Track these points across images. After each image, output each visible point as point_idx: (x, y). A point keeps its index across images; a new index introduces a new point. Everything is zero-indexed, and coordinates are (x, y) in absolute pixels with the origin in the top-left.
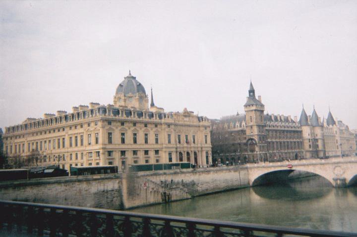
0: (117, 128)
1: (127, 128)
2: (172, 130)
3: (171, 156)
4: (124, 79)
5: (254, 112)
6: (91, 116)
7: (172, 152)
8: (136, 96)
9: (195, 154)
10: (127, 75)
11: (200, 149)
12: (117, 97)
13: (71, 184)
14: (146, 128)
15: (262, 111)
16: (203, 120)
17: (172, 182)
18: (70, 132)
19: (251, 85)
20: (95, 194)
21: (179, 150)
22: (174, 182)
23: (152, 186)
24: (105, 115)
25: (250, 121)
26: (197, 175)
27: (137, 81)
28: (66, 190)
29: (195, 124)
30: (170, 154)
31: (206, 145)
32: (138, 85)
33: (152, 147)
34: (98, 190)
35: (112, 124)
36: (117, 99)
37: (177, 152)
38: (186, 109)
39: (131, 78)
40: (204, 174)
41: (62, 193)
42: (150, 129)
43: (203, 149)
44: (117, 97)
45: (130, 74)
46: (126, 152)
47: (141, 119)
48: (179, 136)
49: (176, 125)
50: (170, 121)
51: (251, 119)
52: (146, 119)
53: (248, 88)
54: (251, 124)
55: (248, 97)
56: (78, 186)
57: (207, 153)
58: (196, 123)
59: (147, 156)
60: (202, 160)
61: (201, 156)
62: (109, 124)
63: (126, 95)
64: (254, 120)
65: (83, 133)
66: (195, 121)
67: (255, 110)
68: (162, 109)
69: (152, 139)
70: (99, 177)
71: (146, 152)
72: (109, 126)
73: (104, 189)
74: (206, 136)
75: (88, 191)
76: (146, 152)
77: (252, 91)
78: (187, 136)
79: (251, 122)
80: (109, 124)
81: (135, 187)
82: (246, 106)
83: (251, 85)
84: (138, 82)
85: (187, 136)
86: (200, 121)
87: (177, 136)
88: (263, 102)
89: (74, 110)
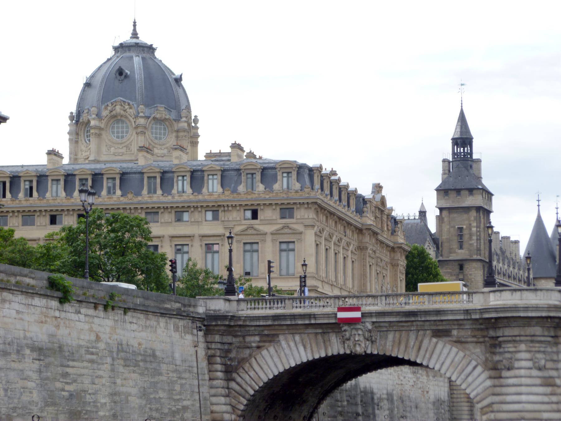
5: (473, 213)
6: (261, 187)
8: (178, 120)
15: (488, 212)
19: (462, 119)
25: (455, 245)
39: (135, 48)
44: (105, 113)
45: (135, 35)
51: (461, 236)
53: (451, 130)
54: (461, 254)
55: (449, 162)
64: (474, 242)
66: (386, 229)
67: (479, 209)
77: (463, 140)
79: (461, 247)
82: (443, 191)
83: (462, 119)
88: (487, 182)
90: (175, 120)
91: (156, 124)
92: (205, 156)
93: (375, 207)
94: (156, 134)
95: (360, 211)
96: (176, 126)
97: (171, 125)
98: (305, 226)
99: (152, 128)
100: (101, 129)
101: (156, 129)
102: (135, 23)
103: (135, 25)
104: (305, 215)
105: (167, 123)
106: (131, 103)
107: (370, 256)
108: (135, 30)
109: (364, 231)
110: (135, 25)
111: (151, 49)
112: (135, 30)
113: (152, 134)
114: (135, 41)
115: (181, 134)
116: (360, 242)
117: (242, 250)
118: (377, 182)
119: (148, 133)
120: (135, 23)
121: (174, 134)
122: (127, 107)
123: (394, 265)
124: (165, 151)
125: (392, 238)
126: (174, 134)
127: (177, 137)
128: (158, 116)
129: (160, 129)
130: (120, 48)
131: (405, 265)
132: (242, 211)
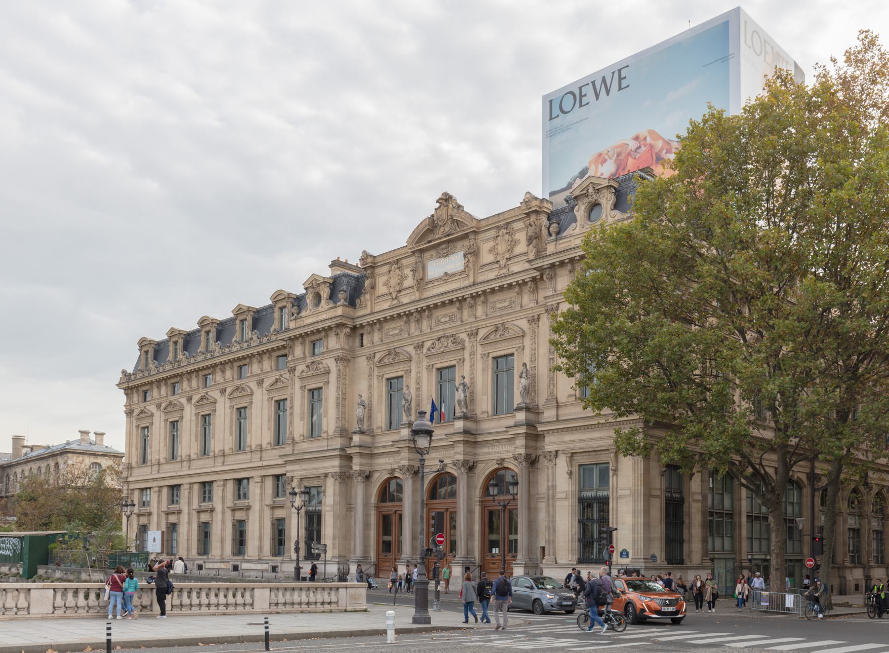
2: (331, 363)
43: (550, 444)
66: (521, 248)
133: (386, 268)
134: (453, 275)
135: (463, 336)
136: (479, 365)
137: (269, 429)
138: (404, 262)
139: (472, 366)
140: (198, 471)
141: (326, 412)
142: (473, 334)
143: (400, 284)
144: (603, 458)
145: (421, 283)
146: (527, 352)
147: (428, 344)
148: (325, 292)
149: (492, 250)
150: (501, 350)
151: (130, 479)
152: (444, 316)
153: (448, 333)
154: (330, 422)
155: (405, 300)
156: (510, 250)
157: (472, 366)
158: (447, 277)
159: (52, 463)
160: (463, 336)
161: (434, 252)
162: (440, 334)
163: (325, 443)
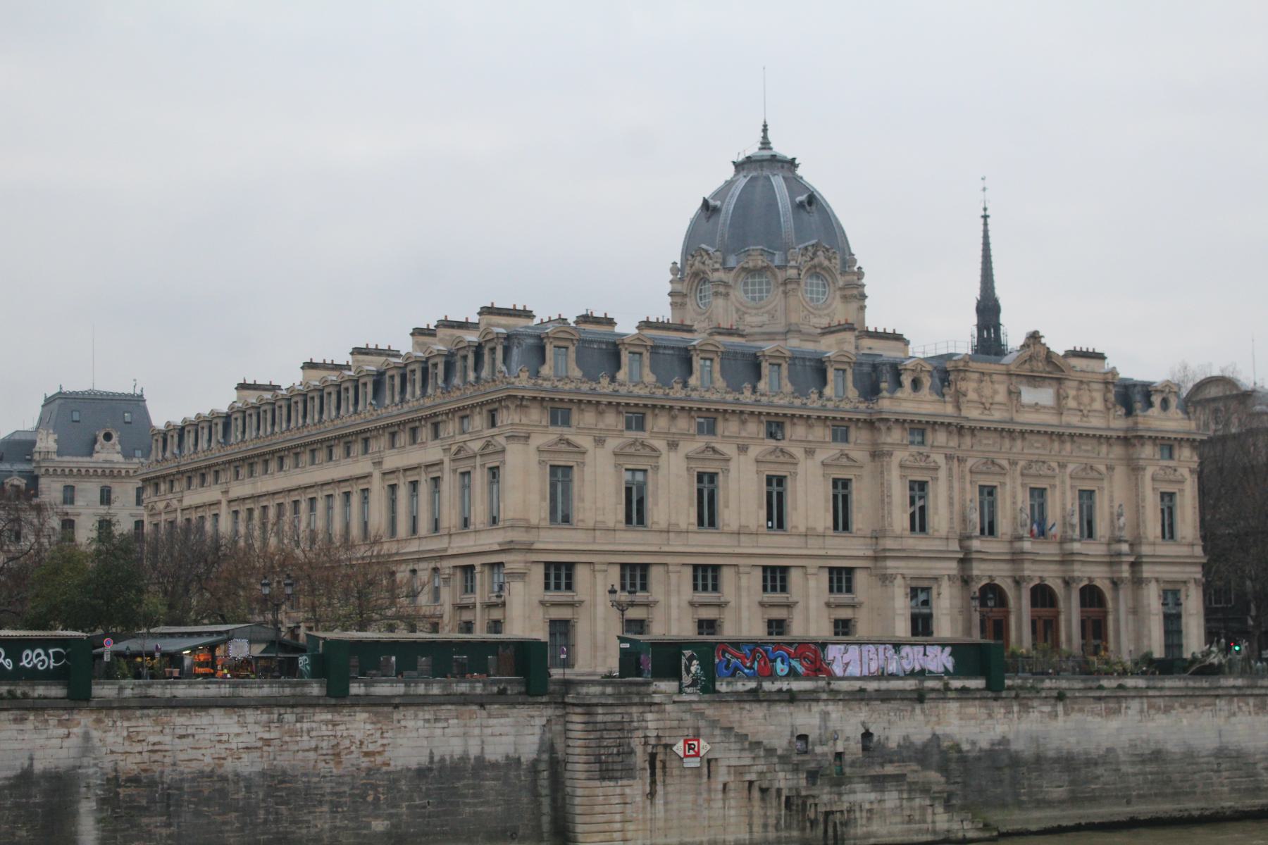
0: (600, 441)
1: (660, 444)
2: (939, 458)
3: (926, 603)
4: (730, 172)
7: (936, 579)
9: (1091, 596)
10: (753, 149)
11: (1125, 572)
12: (687, 270)
13: (289, 717)
14: (773, 443)
16: (1150, 404)
17: (865, 748)
18: (393, 460)
20: (422, 773)
21: (977, 569)
22: (881, 745)
23: (730, 756)
24: (537, 374)
26: (1034, 715)
27: (798, 180)
28: (267, 742)
29: (1096, 422)
30: (920, 592)
31: (1168, 549)
32: (801, 205)
33: (815, 547)
34: (432, 757)
35: (575, 417)
36: (691, 277)
37: (966, 581)
38: (1034, 337)
39: (765, 165)
40: (1076, 716)
41: (246, 757)
42: (798, 452)
43: (1147, 571)
45: (765, 144)
46: (655, 575)
47: (747, 396)
48: (989, 492)
49: (959, 429)
50: (923, 404)
52: (775, 390)
56: (325, 731)
57: (1171, 596)
58: (1100, 416)
59: (778, 597)
60: (1138, 630)
61: (1135, 611)
62: (554, 422)
63: (732, 261)
65: (440, 463)
66: (1098, 405)
68: (897, 337)
69: (809, 503)
70: (436, 690)
71: (776, 577)
72: (559, 430)
73: (466, 753)
74: (1167, 497)
75: (379, 759)
76: (776, 577)
78: (1039, 494)
80: (554, 422)
81: (632, 752)
84: (805, 188)
85: (1039, 494)
86: (1129, 413)
87: (973, 495)
89: (416, 344)
90: (779, 267)
91: (753, 277)
92: (638, 328)
93: (1009, 374)
94: (753, 292)
95: (871, 391)
96: (781, 275)
97: (774, 276)
98: (507, 437)
99: (746, 284)
100: (685, 296)
101: (753, 284)
102: (765, 126)
103: (765, 130)
104: (508, 418)
105: (769, 273)
106: (711, 250)
107: (901, 466)
108: (765, 137)
109: (877, 424)
110: (765, 130)
111: (792, 164)
112: (765, 137)
113: (746, 292)
114: (766, 153)
115: (789, 287)
116: (875, 444)
117: (457, 484)
118: (1032, 329)
119: (738, 294)
120: (765, 126)
121: (781, 289)
122: (706, 257)
123: (1135, 469)
124: (765, 318)
125: (1130, 421)
126: (781, 289)
127: (785, 293)
128: (751, 264)
129: (761, 284)
130: (739, 166)
131: (1195, 466)
132: (457, 420)
133: (975, 376)
134: (1044, 407)
135: (1054, 465)
136: (1069, 494)
137: (827, 510)
138: (995, 377)
139: (1063, 493)
140: (706, 550)
141: (936, 509)
142: (1062, 466)
143: (992, 397)
144: (1178, 587)
145: (1020, 407)
146: (1106, 492)
147: (1022, 463)
148: (927, 381)
149: (1076, 398)
150: (1087, 486)
151: (536, 546)
152: (1037, 441)
153: (1043, 458)
154: (940, 519)
155: (997, 415)
156: (1090, 404)
157: (1063, 493)
158: (1036, 407)
159: (287, 501)
160: (1054, 465)
161: (1024, 380)
162: (1034, 458)
163: (937, 542)
